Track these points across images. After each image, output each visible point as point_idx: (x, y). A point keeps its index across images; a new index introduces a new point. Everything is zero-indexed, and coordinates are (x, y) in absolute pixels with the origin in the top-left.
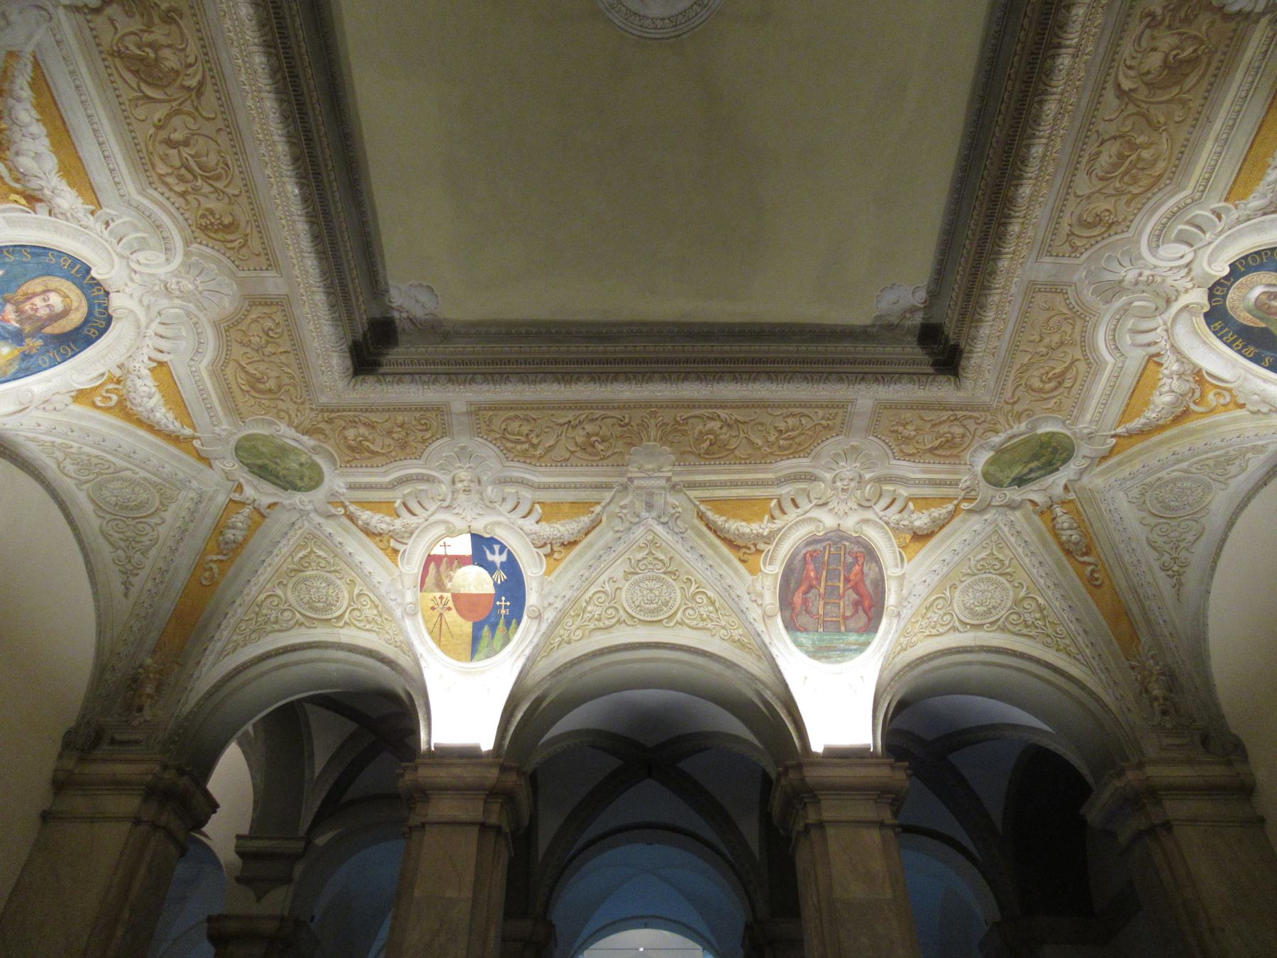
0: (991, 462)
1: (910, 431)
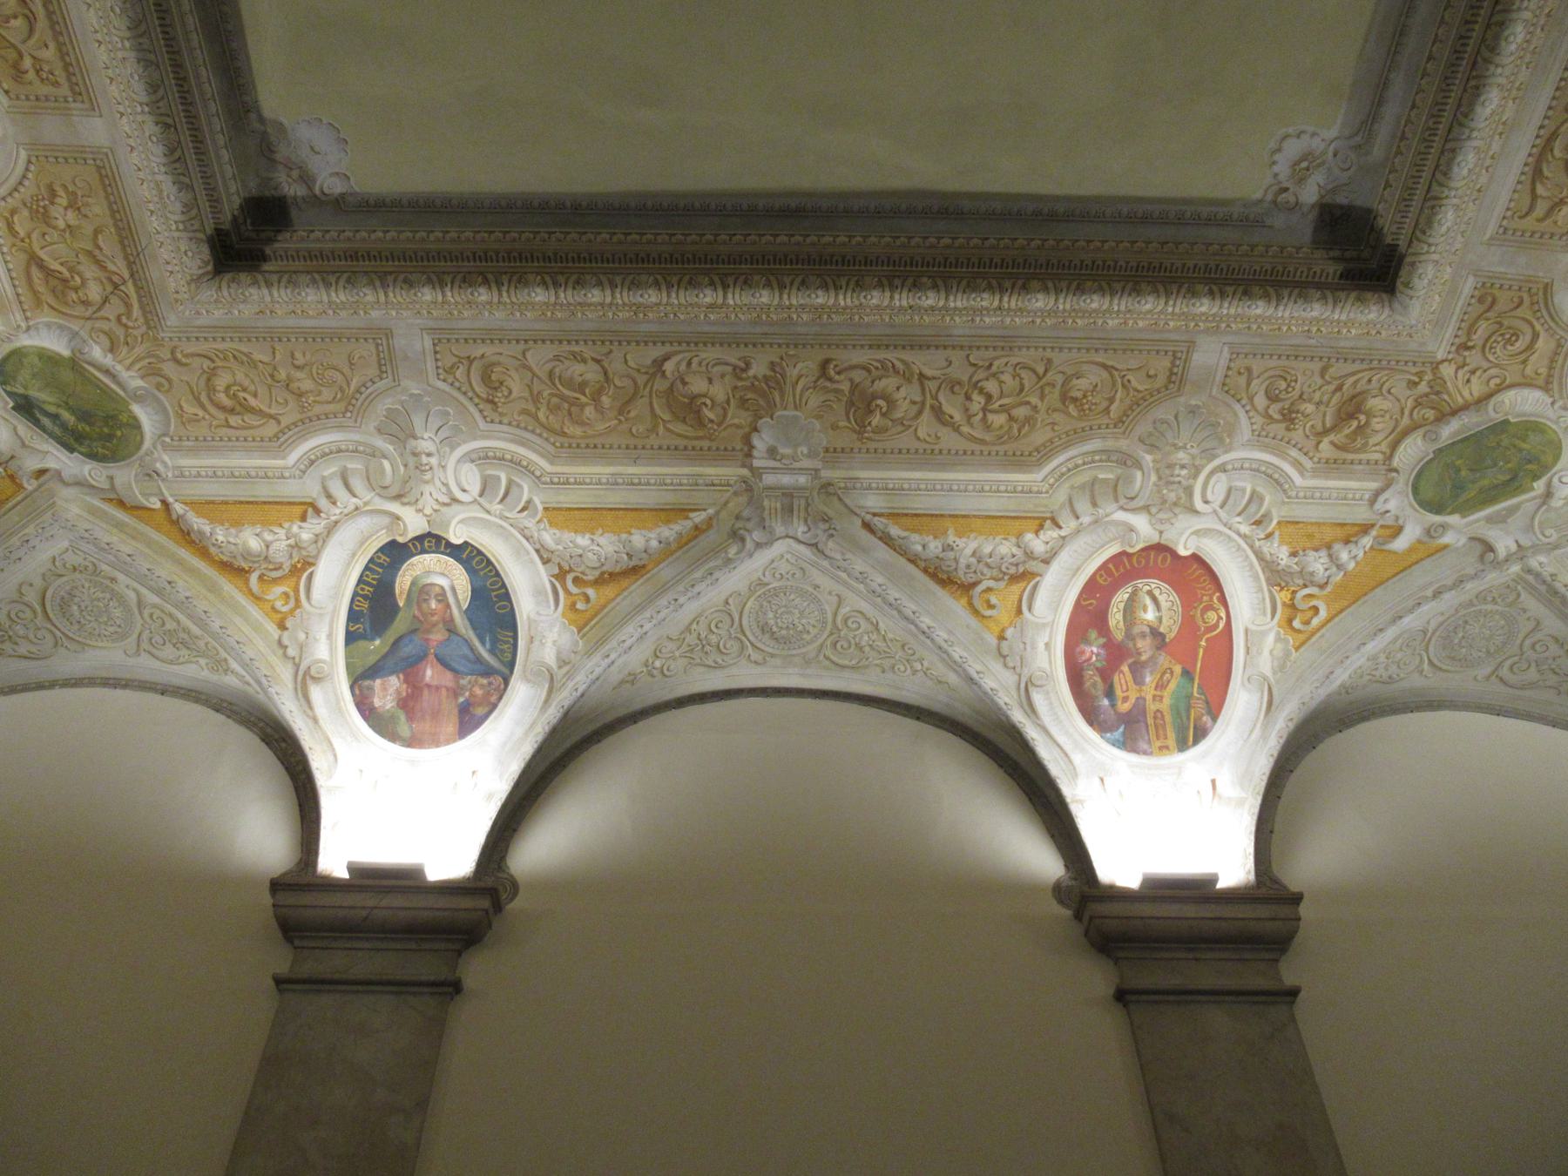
0: (49, 359)
1: (62, 216)
